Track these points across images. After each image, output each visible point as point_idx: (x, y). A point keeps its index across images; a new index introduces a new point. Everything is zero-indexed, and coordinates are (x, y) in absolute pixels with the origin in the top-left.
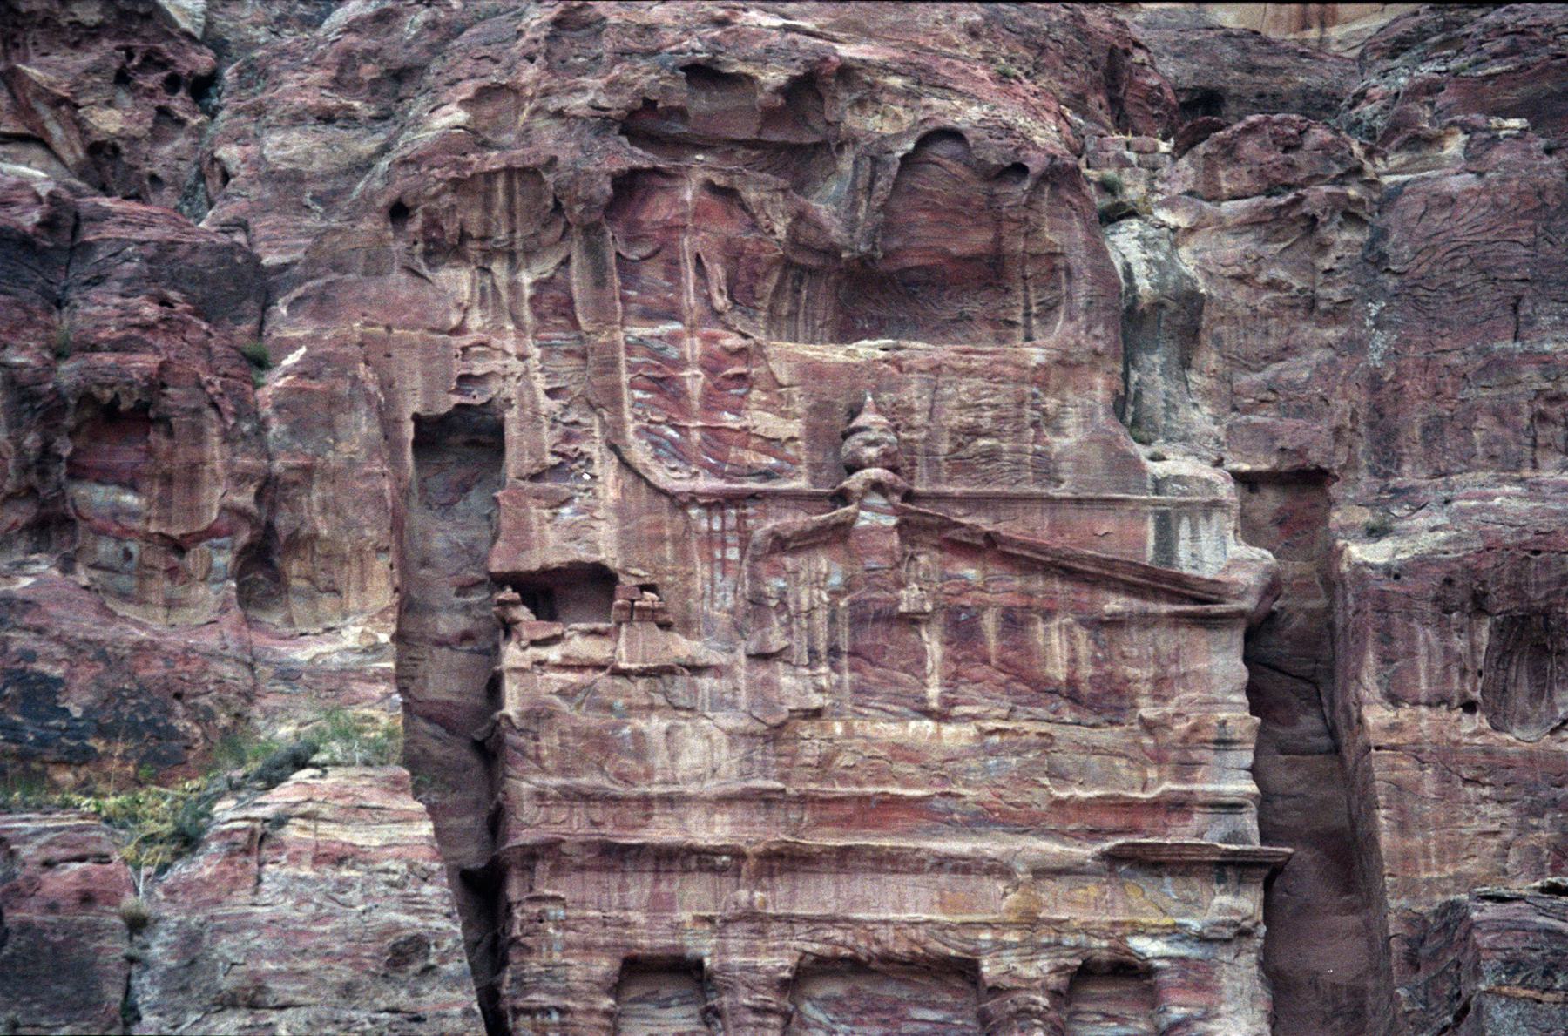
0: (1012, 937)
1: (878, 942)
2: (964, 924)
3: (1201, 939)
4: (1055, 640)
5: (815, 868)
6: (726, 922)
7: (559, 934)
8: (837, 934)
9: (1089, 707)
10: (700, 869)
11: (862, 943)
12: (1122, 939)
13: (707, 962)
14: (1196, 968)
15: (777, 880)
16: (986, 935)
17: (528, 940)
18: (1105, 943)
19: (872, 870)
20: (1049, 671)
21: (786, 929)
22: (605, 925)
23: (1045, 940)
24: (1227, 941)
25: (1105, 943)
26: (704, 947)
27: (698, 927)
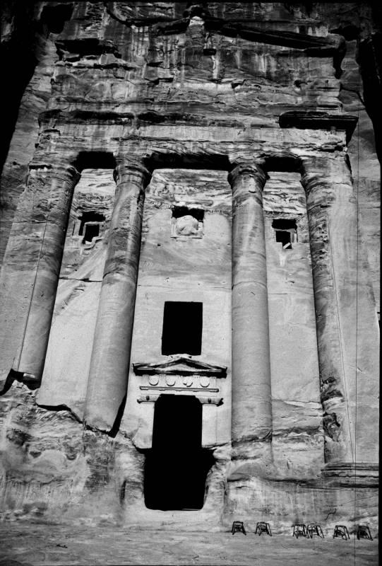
0: (242, 146)
1: (186, 148)
2: (222, 142)
3: (321, 150)
4: (262, 60)
5: (163, 124)
6: (123, 140)
7: (55, 143)
8: (169, 145)
9: (275, 81)
10: (116, 124)
11: (179, 149)
12: (288, 149)
13: (114, 154)
14: (319, 160)
15: (147, 127)
16: (231, 146)
17: (41, 145)
18: (281, 151)
19: (185, 124)
20: (260, 70)
21: (148, 143)
22: (74, 141)
23: (256, 148)
24: (331, 151)
25: (281, 151)
26: (113, 148)
27: (112, 142)
